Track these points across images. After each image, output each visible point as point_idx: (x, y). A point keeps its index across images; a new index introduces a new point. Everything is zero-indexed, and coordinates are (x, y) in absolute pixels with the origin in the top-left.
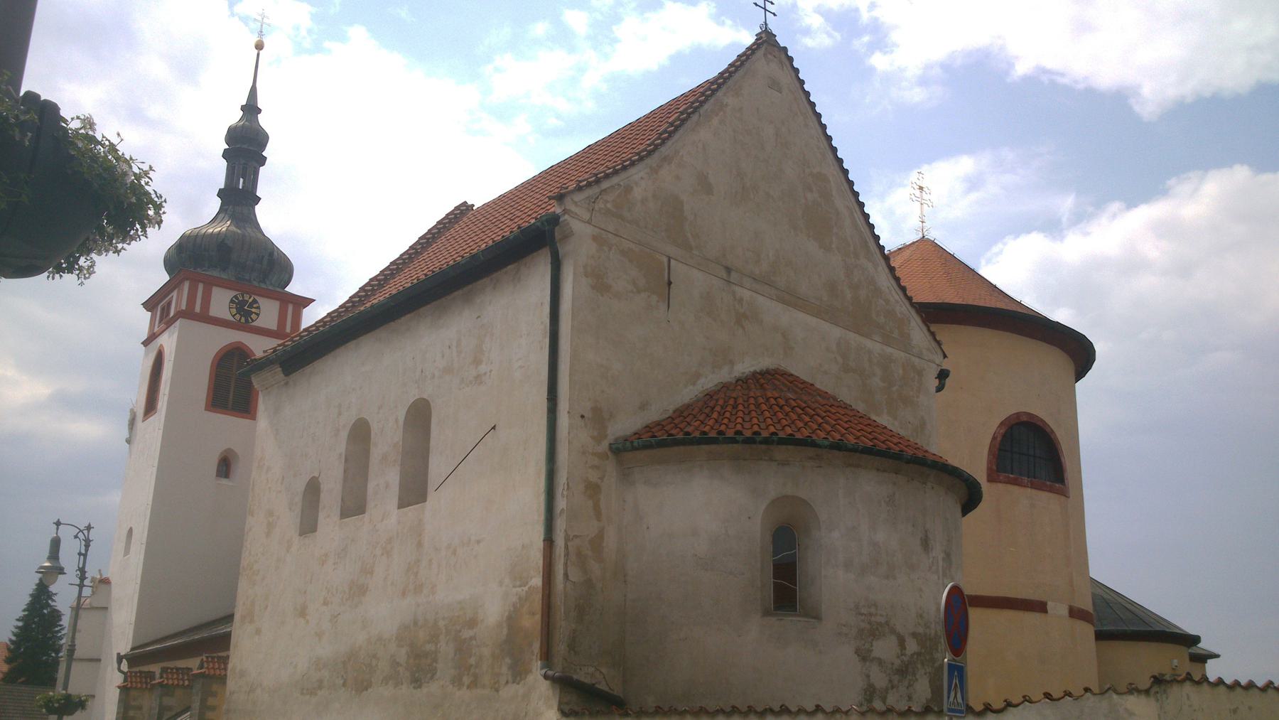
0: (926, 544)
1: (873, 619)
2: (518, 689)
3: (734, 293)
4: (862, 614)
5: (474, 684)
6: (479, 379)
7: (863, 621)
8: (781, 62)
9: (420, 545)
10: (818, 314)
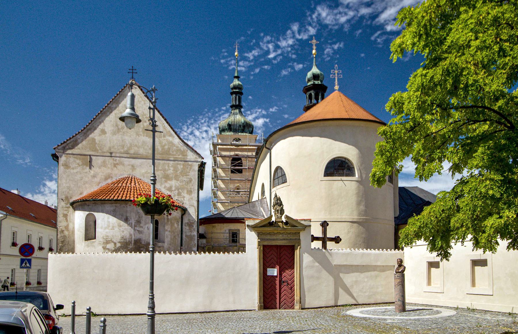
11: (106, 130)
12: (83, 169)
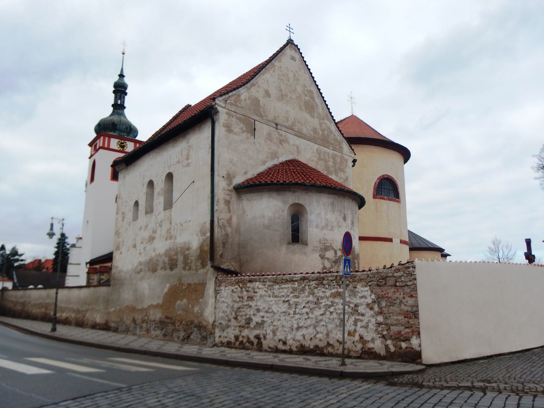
0: (345, 219)
1: (326, 244)
2: (204, 270)
3: (279, 133)
4: (322, 243)
5: (190, 269)
6: (188, 165)
7: (322, 245)
8: (296, 50)
9: (171, 223)
10: (309, 140)
11: (270, 92)
12: (247, 138)
